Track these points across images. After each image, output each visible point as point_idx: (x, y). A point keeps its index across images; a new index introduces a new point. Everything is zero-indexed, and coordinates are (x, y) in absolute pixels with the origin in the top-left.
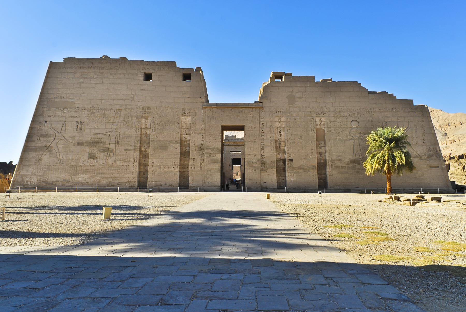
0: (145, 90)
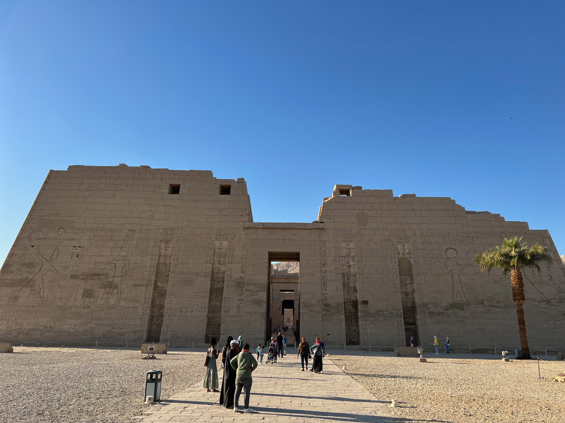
0: (169, 206)
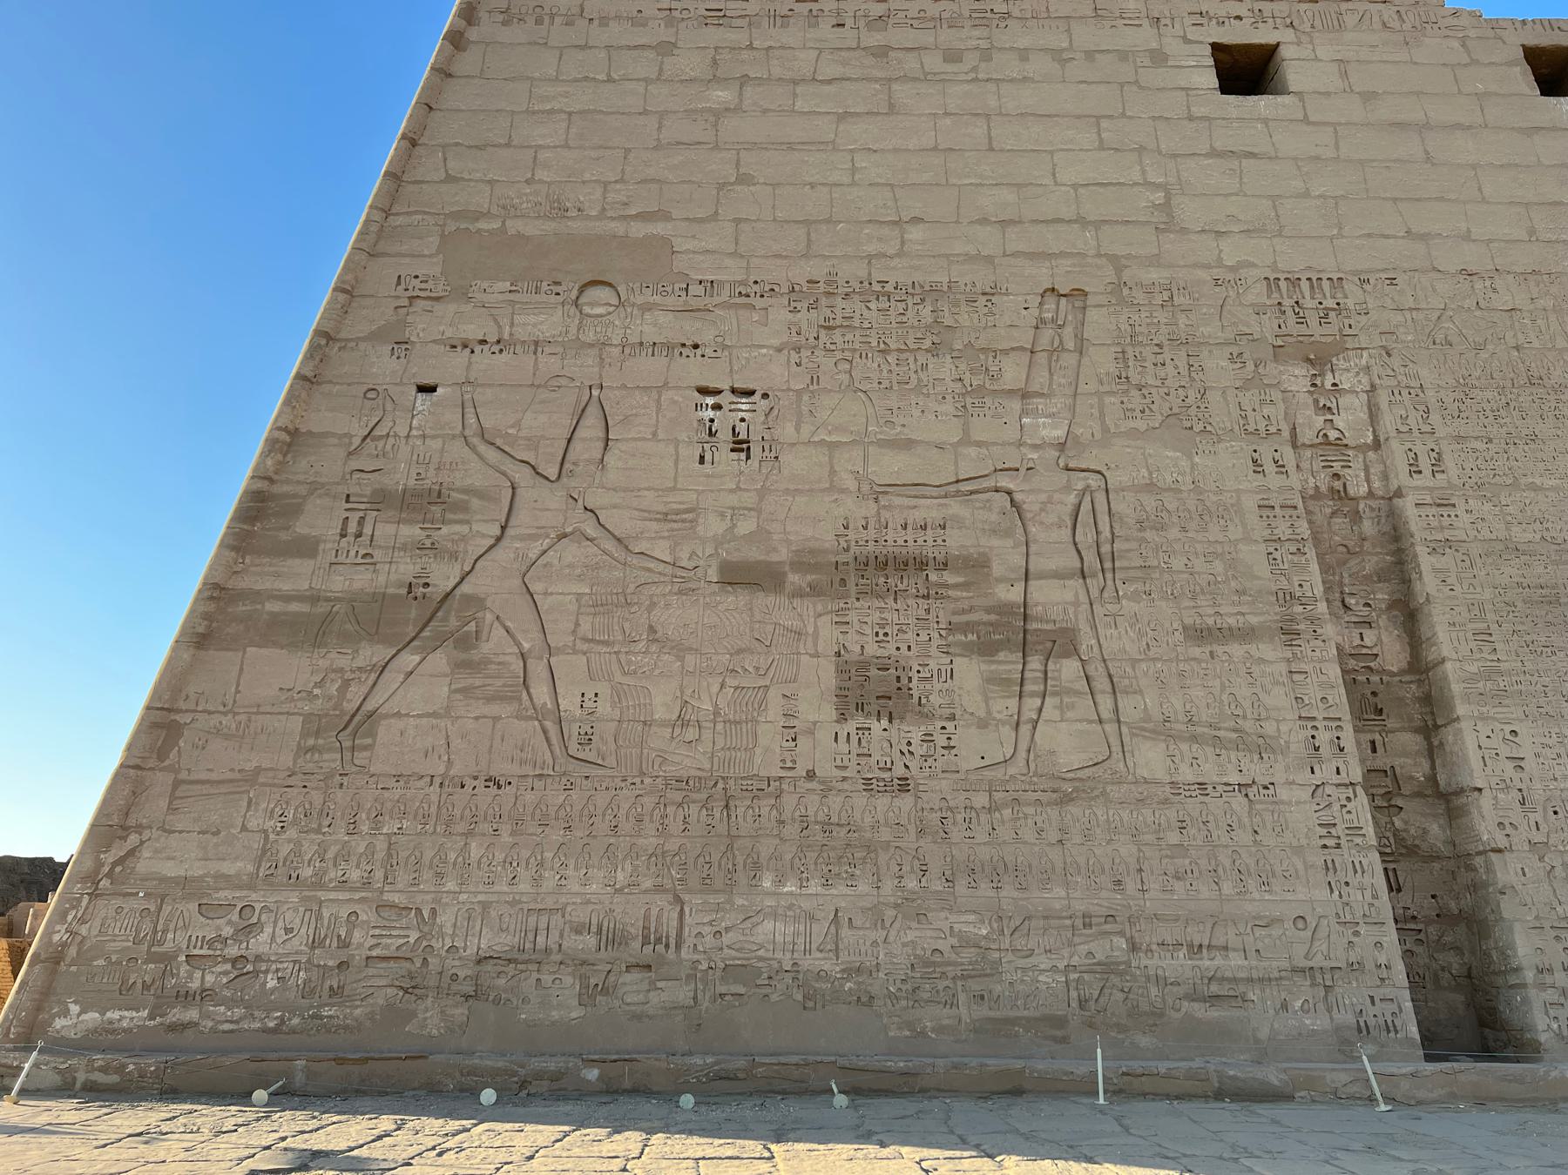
0: (1252, 155)
